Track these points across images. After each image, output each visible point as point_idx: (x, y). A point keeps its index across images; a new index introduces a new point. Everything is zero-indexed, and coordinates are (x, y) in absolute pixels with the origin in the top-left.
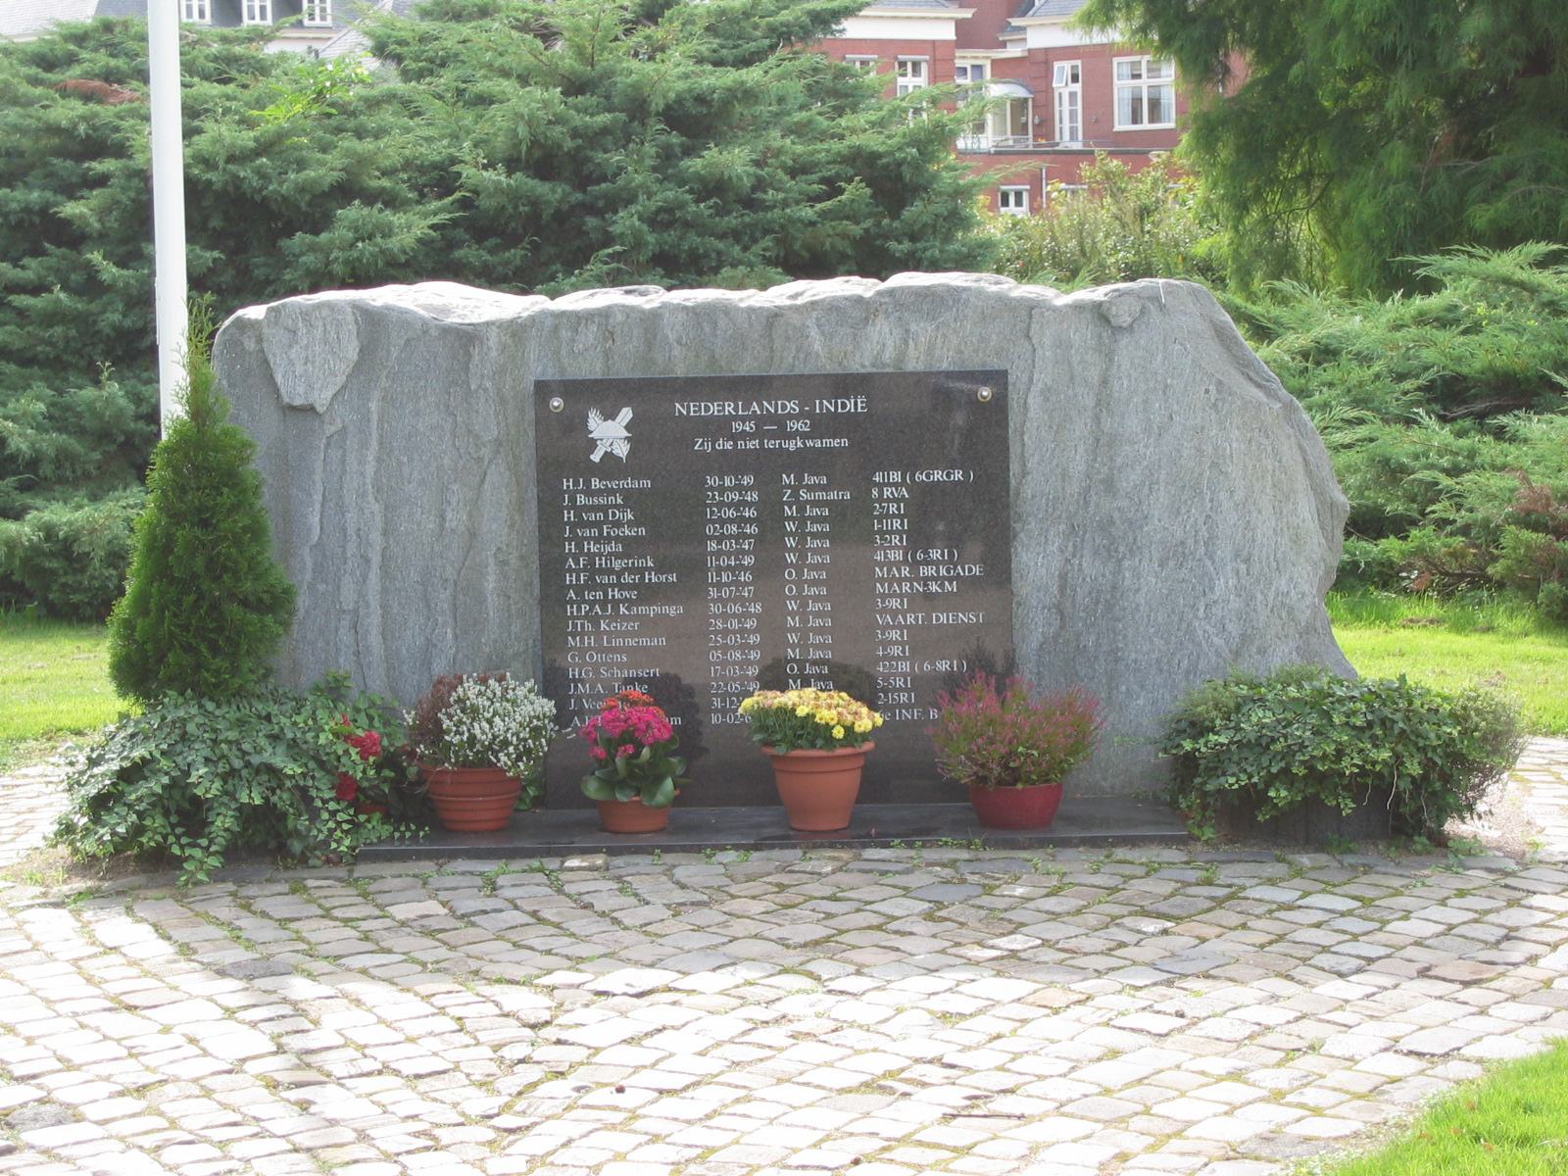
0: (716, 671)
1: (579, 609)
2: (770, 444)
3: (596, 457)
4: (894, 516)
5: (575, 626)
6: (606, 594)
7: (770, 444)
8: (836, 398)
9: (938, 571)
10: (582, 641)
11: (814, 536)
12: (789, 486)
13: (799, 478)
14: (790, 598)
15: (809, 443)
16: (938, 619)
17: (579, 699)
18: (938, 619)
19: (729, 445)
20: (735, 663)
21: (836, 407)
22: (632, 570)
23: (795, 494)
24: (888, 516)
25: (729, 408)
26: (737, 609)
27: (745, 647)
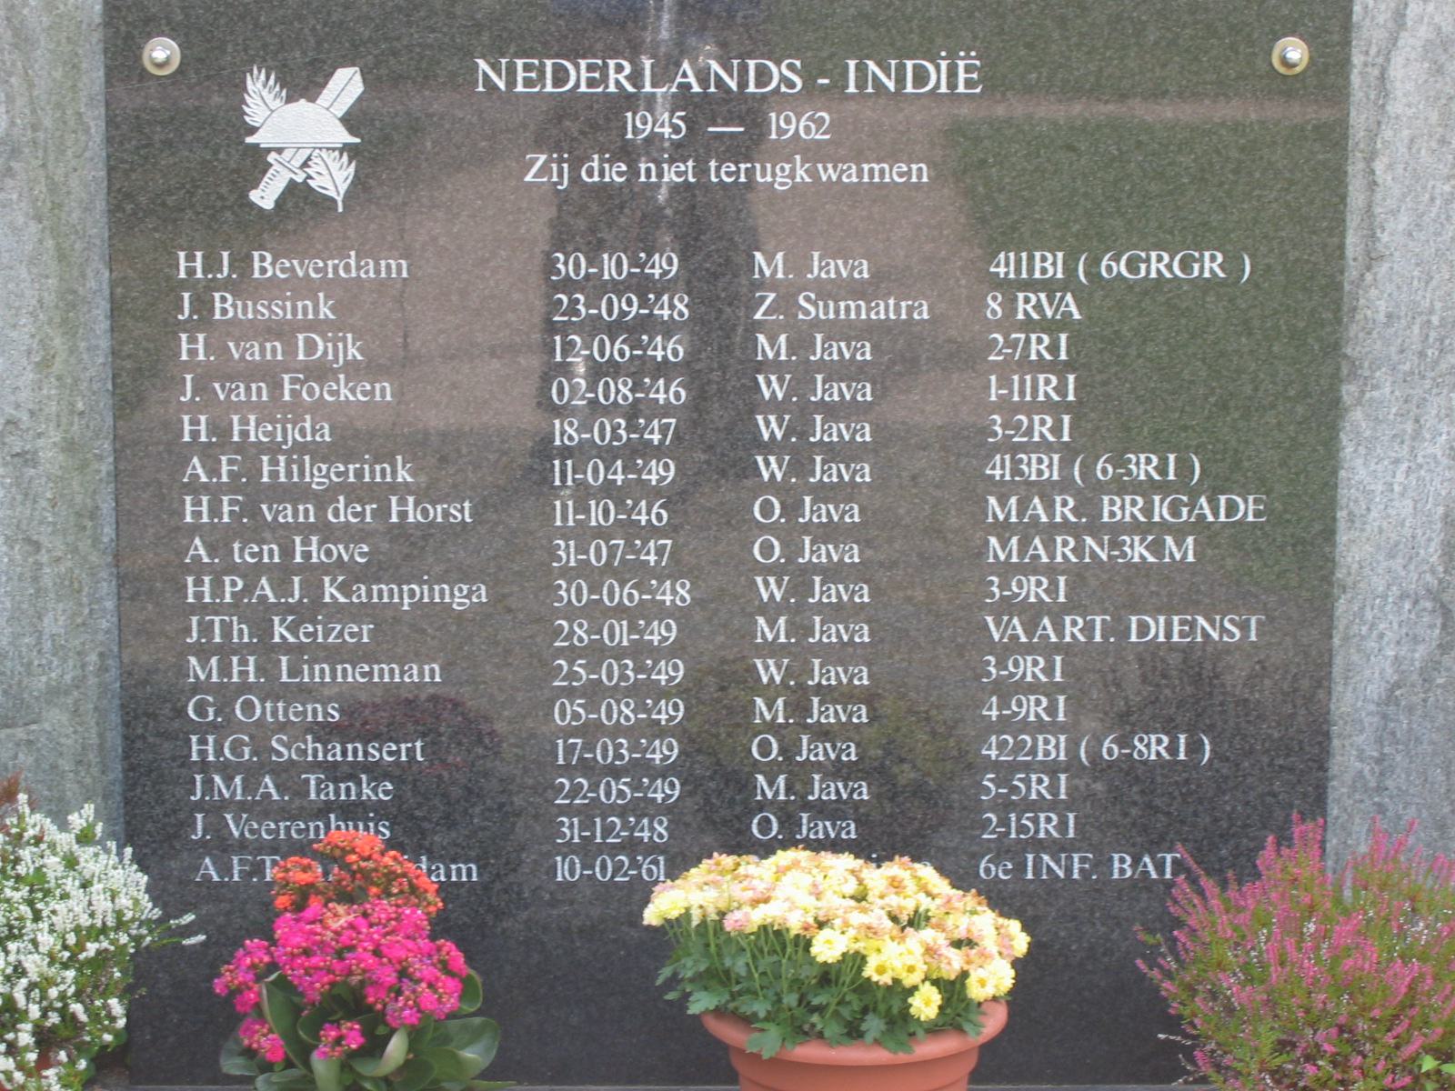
0: (570, 750)
1: (218, 587)
3: (265, 196)
4: (1041, 366)
5: (206, 629)
6: (287, 552)
8: (903, 54)
9: (1147, 510)
10: (225, 670)
11: (832, 412)
13: (798, 264)
14: (767, 571)
15: (828, 173)
17: (216, 810)
19: (615, 174)
20: (617, 730)
21: (900, 81)
22: (357, 493)
23: (787, 302)
26: (626, 594)
27: (644, 692)
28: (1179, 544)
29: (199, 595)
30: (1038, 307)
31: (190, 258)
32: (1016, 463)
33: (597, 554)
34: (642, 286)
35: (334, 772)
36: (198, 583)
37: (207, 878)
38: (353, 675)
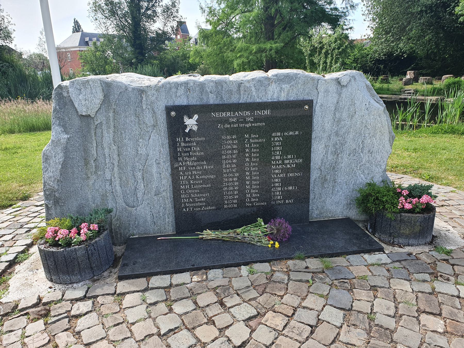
0: (225, 193)
1: (184, 177)
2: (241, 125)
3: (187, 131)
4: (278, 146)
5: (183, 182)
6: (192, 173)
7: (241, 125)
8: (262, 110)
9: (290, 162)
10: (185, 187)
11: (254, 153)
12: (247, 138)
13: (250, 136)
14: (247, 171)
15: (253, 125)
16: (289, 175)
17: (185, 203)
18: (289, 175)
19: (229, 126)
20: (231, 191)
21: (261, 113)
22: (199, 165)
23: (249, 140)
24: (276, 146)
25: (228, 114)
26: (231, 175)
27: (233, 186)
28: (293, 165)
29: (182, 179)
30: (277, 139)
31: (178, 139)
32: (275, 157)
33: (228, 171)
34: (232, 139)
35: (198, 198)
36: (181, 177)
37: (184, 211)
38: (200, 186)
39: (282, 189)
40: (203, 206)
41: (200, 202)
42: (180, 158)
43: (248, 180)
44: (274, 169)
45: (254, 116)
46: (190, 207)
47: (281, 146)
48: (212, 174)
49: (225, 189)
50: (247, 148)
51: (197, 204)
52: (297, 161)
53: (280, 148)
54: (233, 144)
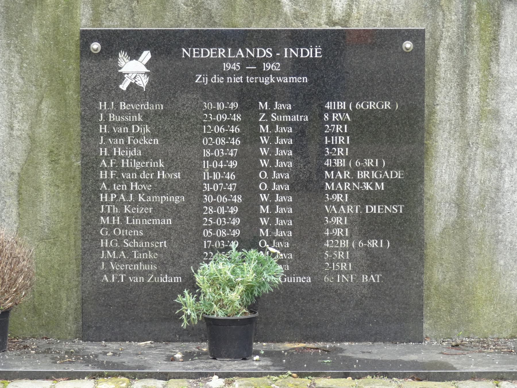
0: (208, 244)
1: (109, 196)
2: (250, 80)
3: (124, 87)
4: (340, 134)
5: (106, 209)
6: (128, 187)
7: (250, 80)
8: (300, 47)
10: (111, 221)
11: (281, 147)
12: (264, 111)
13: (272, 105)
15: (279, 80)
16: (370, 209)
17: (108, 261)
18: (370, 209)
19: (221, 80)
22: (148, 170)
23: (268, 116)
24: (335, 134)
25: (221, 52)
26: (224, 199)
27: (229, 227)
28: (380, 185)
29: (104, 199)
30: (339, 117)
31: (103, 104)
32: (333, 161)
33: (215, 187)
34: (227, 111)
35: (141, 250)
36: (104, 195)
37: (105, 281)
38: (147, 222)
39: (350, 245)
40: (150, 272)
41: (146, 261)
42: (103, 150)
43: (264, 215)
44: (331, 193)
45: (281, 59)
46: (120, 272)
47: (347, 134)
48: (175, 193)
49: (207, 232)
50: (262, 134)
51: (136, 267)
52: (389, 176)
53: (346, 139)
54: (230, 122)
